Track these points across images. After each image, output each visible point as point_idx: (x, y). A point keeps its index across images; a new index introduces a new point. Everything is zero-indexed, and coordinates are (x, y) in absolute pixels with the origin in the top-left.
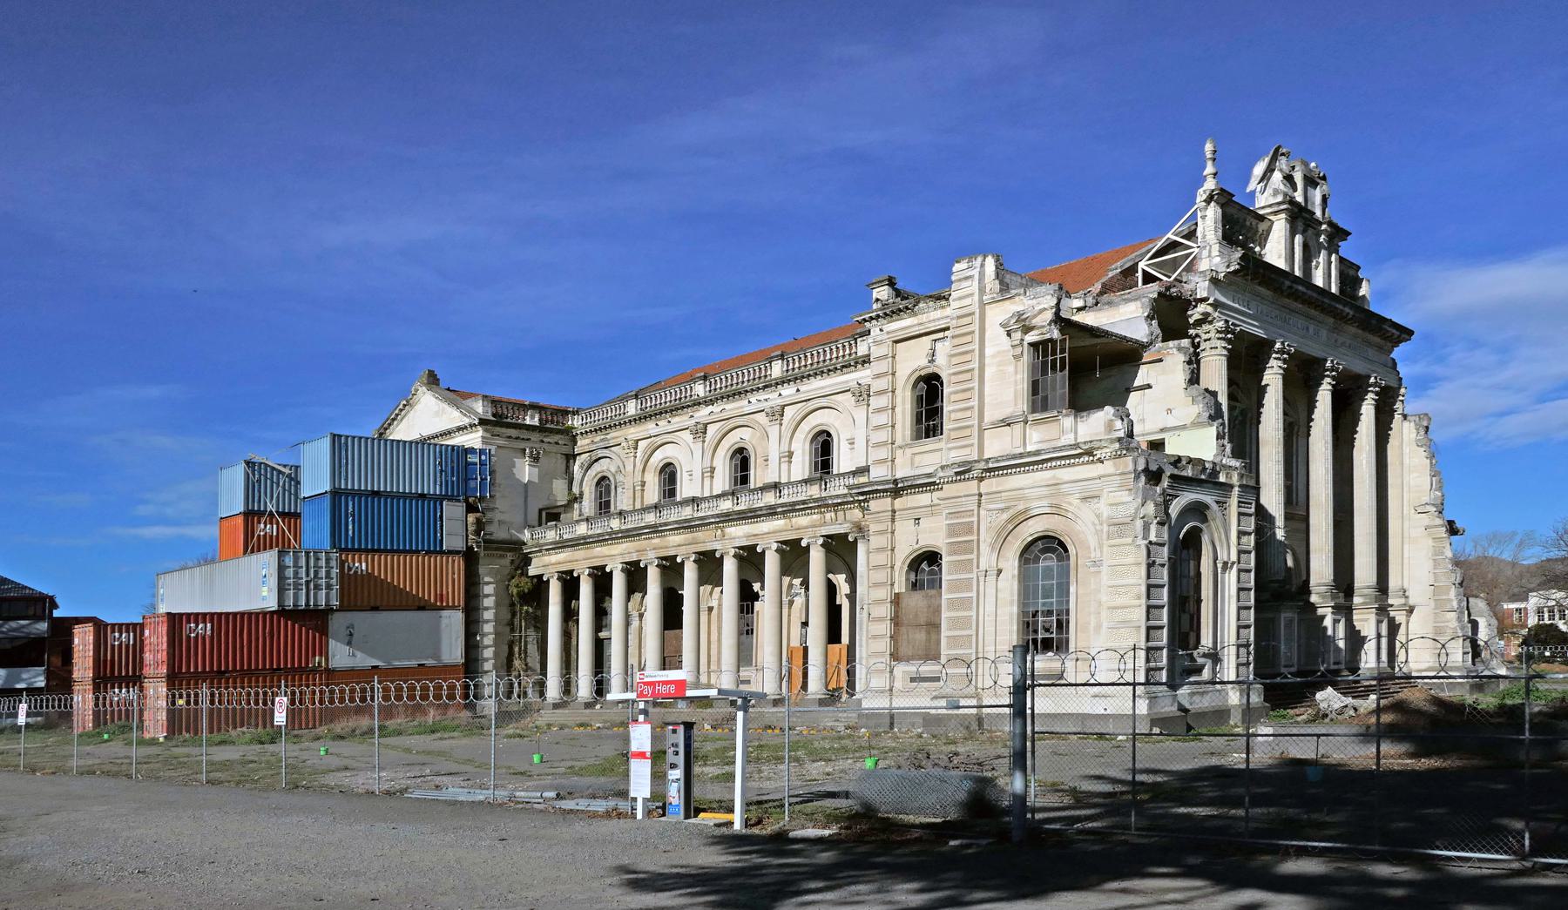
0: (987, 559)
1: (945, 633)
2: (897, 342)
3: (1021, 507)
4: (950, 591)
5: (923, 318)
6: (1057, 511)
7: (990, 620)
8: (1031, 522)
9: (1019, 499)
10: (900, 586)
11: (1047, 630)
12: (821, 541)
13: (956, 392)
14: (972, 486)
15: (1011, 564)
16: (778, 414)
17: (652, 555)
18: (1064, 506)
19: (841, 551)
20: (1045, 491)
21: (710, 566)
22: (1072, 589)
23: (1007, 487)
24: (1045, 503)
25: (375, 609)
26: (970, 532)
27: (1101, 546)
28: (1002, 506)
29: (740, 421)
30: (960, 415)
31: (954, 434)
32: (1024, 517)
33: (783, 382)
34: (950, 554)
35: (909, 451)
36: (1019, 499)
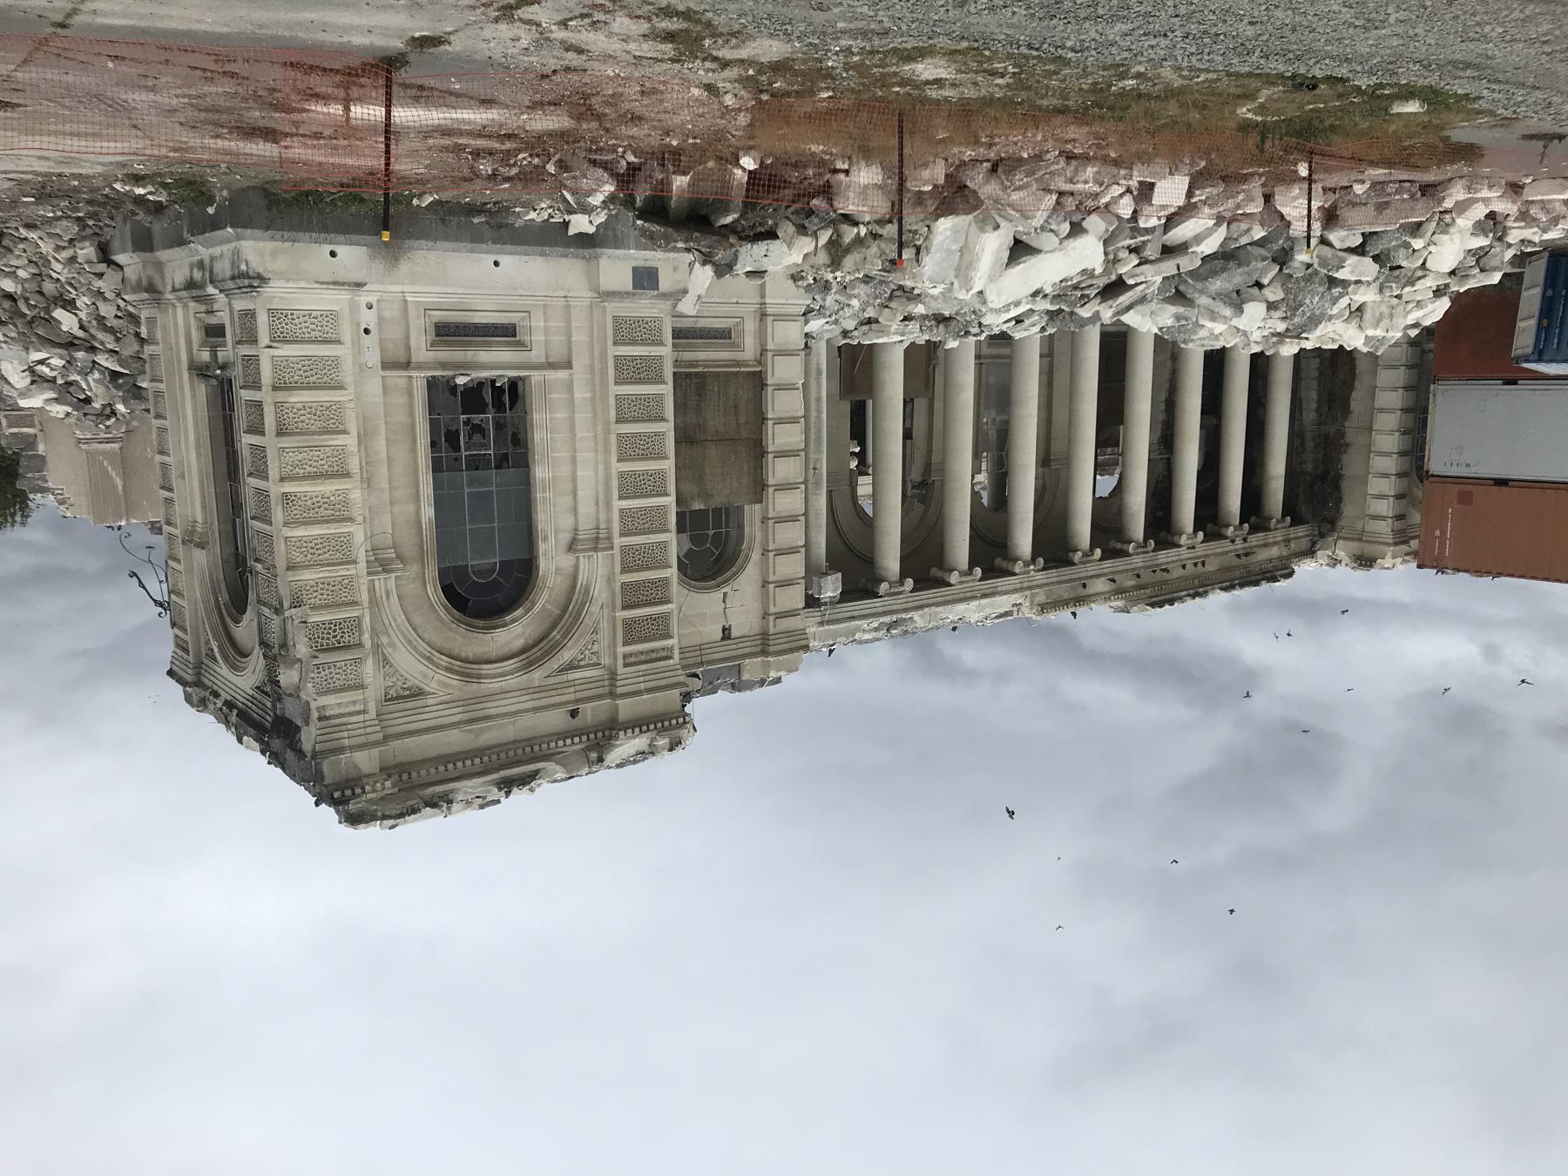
0: (600, 574)
3: (537, 676)
4: (662, 510)
6: (467, 668)
7: (586, 455)
8: (519, 643)
9: (541, 689)
10: (752, 512)
11: (478, 429)
12: (884, 587)
15: (552, 561)
17: (1138, 561)
18: (453, 681)
20: (492, 708)
22: (428, 512)
25: (1502, 482)
26: (628, 625)
27: (374, 602)
32: (534, 653)
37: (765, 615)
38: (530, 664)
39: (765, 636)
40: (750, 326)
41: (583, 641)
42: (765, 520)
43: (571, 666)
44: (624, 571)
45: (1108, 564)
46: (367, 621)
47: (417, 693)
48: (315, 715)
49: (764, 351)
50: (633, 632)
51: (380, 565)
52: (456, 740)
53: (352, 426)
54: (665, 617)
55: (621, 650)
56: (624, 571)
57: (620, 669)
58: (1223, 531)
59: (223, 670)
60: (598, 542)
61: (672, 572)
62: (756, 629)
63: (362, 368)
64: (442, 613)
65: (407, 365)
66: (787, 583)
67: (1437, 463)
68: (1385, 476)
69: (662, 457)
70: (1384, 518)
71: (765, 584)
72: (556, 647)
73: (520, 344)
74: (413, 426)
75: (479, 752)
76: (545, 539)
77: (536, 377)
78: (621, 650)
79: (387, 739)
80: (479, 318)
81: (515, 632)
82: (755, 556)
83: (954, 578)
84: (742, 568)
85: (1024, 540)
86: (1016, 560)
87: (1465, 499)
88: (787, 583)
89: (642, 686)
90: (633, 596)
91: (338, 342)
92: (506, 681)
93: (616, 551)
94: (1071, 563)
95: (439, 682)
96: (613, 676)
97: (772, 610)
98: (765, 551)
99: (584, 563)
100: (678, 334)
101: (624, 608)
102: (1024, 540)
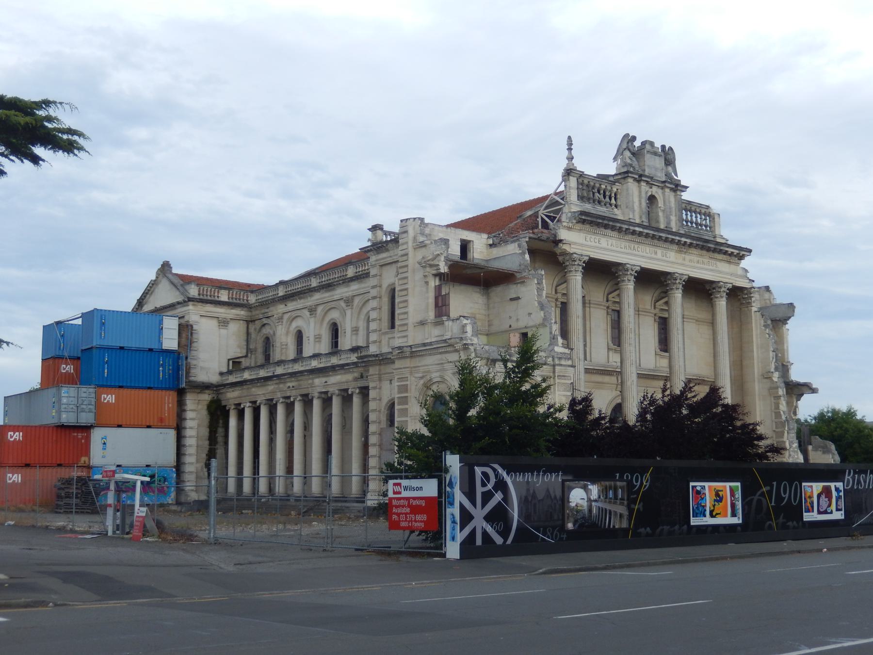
2: (381, 266)
3: (428, 378)
5: (391, 253)
12: (357, 391)
14: (407, 363)
16: (349, 301)
17: (279, 395)
21: (307, 401)
24: (437, 374)
28: (421, 375)
29: (333, 304)
31: (401, 329)
33: (352, 279)
34: (399, 404)
37: (380, 388)
39: (380, 380)
42: (379, 423)
44: (407, 409)
45: (288, 395)
54: (399, 392)
55: (408, 383)
56: (407, 409)
61: (397, 407)
66: (374, 399)
70: (191, 419)
71: (380, 400)
75: (441, 353)
78: (408, 383)
83: (337, 392)
85: (317, 404)
88: (374, 399)
90: (404, 400)
92: (436, 377)
96: (411, 373)
98: (379, 411)
102: (317, 404)
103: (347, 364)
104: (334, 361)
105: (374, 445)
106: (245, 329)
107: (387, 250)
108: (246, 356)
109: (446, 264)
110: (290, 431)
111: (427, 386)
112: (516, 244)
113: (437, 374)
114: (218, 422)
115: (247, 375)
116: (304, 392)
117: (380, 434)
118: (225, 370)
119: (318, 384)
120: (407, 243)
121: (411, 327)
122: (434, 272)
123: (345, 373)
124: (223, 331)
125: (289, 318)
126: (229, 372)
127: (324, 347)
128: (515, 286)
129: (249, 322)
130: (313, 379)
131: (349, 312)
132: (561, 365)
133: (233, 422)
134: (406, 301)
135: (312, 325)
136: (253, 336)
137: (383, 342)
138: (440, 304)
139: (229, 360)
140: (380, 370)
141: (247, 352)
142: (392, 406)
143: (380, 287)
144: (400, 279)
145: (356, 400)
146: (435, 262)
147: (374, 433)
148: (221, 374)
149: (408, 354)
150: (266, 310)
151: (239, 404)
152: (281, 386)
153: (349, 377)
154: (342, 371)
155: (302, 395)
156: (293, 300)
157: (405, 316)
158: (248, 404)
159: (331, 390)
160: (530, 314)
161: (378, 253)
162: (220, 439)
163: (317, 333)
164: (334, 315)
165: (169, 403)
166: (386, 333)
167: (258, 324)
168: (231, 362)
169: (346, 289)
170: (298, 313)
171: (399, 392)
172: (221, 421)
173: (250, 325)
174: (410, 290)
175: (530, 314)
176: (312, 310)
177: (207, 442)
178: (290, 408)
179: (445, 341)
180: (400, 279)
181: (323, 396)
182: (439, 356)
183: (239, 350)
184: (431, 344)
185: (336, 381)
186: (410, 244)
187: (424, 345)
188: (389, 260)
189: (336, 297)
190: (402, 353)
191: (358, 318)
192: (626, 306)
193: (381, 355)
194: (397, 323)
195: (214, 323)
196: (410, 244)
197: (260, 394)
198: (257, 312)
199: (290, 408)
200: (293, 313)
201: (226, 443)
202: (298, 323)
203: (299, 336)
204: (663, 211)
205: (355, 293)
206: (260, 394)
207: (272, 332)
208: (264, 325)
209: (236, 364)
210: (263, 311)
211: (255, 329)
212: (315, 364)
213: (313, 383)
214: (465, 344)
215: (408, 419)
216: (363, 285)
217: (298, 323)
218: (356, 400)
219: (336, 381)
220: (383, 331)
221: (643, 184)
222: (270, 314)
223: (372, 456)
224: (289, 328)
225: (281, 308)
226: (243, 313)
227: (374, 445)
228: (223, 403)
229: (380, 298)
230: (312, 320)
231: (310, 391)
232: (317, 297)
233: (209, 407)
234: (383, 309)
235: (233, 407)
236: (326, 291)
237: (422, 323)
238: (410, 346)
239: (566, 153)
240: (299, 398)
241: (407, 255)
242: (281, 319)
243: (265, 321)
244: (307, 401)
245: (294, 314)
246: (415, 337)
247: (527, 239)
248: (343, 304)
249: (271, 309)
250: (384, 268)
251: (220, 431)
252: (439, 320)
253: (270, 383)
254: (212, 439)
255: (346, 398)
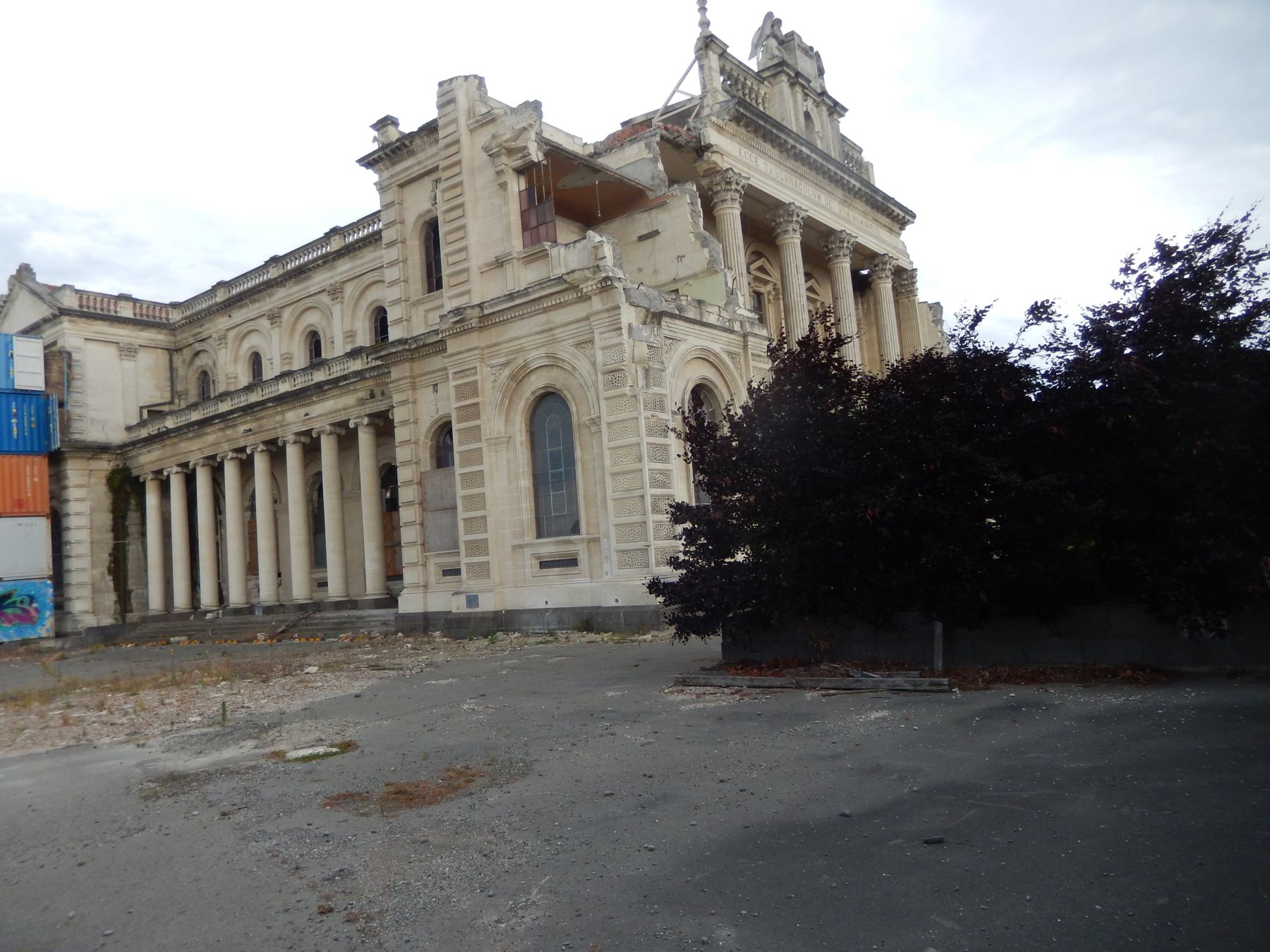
0: (492, 423)
1: (461, 514)
2: (401, 186)
3: (520, 362)
4: (463, 466)
6: (554, 362)
8: (533, 378)
12: (366, 421)
13: (450, 232)
14: (474, 340)
17: (226, 447)
18: (561, 354)
19: (383, 426)
20: (541, 338)
21: (276, 453)
22: (578, 454)
23: (506, 337)
24: (542, 352)
28: (503, 360)
29: (309, 303)
30: (455, 258)
31: (454, 281)
34: (459, 421)
35: (422, 308)
36: (517, 351)
37: (415, 402)
38: (524, 366)
39: (414, 387)
40: (432, 579)
41: (498, 383)
43: (505, 365)
44: (478, 427)
45: (242, 444)
46: (601, 387)
47: (579, 345)
48: (625, 331)
49: (424, 565)
50: (473, 389)
51: (596, 422)
52: (559, 317)
53: (610, 504)
54: (458, 399)
55: (478, 377)
56: (478, 427)
57: (478, 365)
58: (179, 469)
59: (717, 348)
60: (495, 442)
61: (455, 426)
62: (419, 392)
63: (608, 537)
64: (568, 396)
65: (589, 541)
67: (42, 526)
68: (78, 514)
69: (464, 497)
71: (416, 422)
72: (512, 377)
73: (537, 558)
74: (586, 506)
75: (546, 310)
76: (522, 443)
77: (530, 537)
78: (478, 377)
79: (587, 318)
80: (556, 570)
81: (536, 383)
82: (422, 438)
84: (429, 430)
85: (293, 455)
86: (295, 442)
87: (20, 503)
89: (466, 355)
90: (472, 412)
91: (618, 551)
92: (536, 356)
93: (484, 438)
94: (265, 443)
95: (566, 351)
97: (410, 406)
99: (503, 430)
100: (457, 572)
101: (477, 404)
102: (293, 455)
103: (345, 377)
104: (319, 376)
105: (410, 503)
106: (167, 363)
107: (412, 153)
108: (171, 403)
109: (540, 148)
110: (249, 507)
111: (519, 377)
112: (642, 143)
113: (542, 352)
114: (127, 502)
115: (170, 423)
116: (269, 436)
117: (420, 483)
118: (134, 421)
119: (293, 420)
120: (455, 120)
121: (475, 275)
122: (518, 163)
123: (340, 395)
124: (129, 364)
125: (236, 336)
126: (142, 424)
127: (300, 360)
128: (645, 215)
129: (172, 351)
130: (283, 412)
131: (336, 310)
132: (755, 335)
133: (152, 500)
134: (463, 227)
135: (276, 339)
136: (181, 371)
137: (414, 320)
138: (533, 223)
139: (141, 408)
140: (412, 370)
141: (172, 397)
142: (444, 430)
143: (402, 222)
144: (444, 191)
145: (365, 439)
146: (520, 143)
147: (408, 483)
148: (129, 429)
149: (474, 322)
150: (199, 330)
151: (160, 472)
152: (229, 432)
153: (349, 400)
154: (336, 392)
155: (265, 443)
156: (241, 307)
157: (463, 255)
158: (175, 469)
159: (316, 426)
160: (681, 257)
161: (393, 164)
162: (133, 529)
163: (284, 350)
164: (313, 319)
165: (33, 476)
166: (419, 302)
167: (187, 353)
168: (145, 412)
169: (329, 274)
170: (251, 326)
171: (458, 399)
172: (133, 502)
173: (175, 357)
174: (468, 207)
175: (681, 257)
176: (274, 317)
177: (111, 535)
178: (246, 467)
179: (560, 279)
180: (444, 191)
181: (303, 439)
182: (542, 318)
183: (158, 394)
184: (526, 292)
185: (322, 412)
186: (463, 121)
187: (511, 296)
188: (417, 171)
189: (313, 290)
190: (460, 321)
191: (353, 316)
192: (794, 270)
193: (415, 339)
194: (445, 271)
195: (112, 351)
196: (463, 121)
197: (194, 449)
198: (185, 335)
199: (246, 467)
200: (243, 327)
201: (143, 534)
202: (253, 341)
203: (256, 361)
204: (821, 138)
205: (345, 277)
206: (194, 449)
207: (211, 363)
208: (197, 354)
209: (154, 413)
210: (195, 331)
211: (184, 362)
212: (284, 387)
213: (284, 420)
214: (607, 278)
215: (483, 445)
216: (358, 262)
217: (253, 341)
218: (365, 439)
219: (322, 412)
220: (413, 299)
221: (798, 89)
222: (205, 335)
223: (407, 524)
224: (237, 352)
225: (222, 322)
226: (160, 337)
227: (410, 503)
228: (135, 473)
229: (403, 242)
230: (275, 333)
231: (279, 432)
232: (281, 295)
233: (111, 480)
234: (409, 262)
235: (150, 477)
236: (296, 283)
237: (499, 263)
238: (480, 306)
239: (698, 17)
240: (261, 447)
241: (457, 142)
242: (223, 338)
243: (198, 347)
244: (276, 453)
245: (244, 328)
246: (484, 289)
247: (658, 139)
248: (325, 298)
249: (206, 326)
250: (408, 189)
251: (133, 516)
252: (536, 249)
253: (209, 429)
254: (119, 529)
255: (346, 438)
